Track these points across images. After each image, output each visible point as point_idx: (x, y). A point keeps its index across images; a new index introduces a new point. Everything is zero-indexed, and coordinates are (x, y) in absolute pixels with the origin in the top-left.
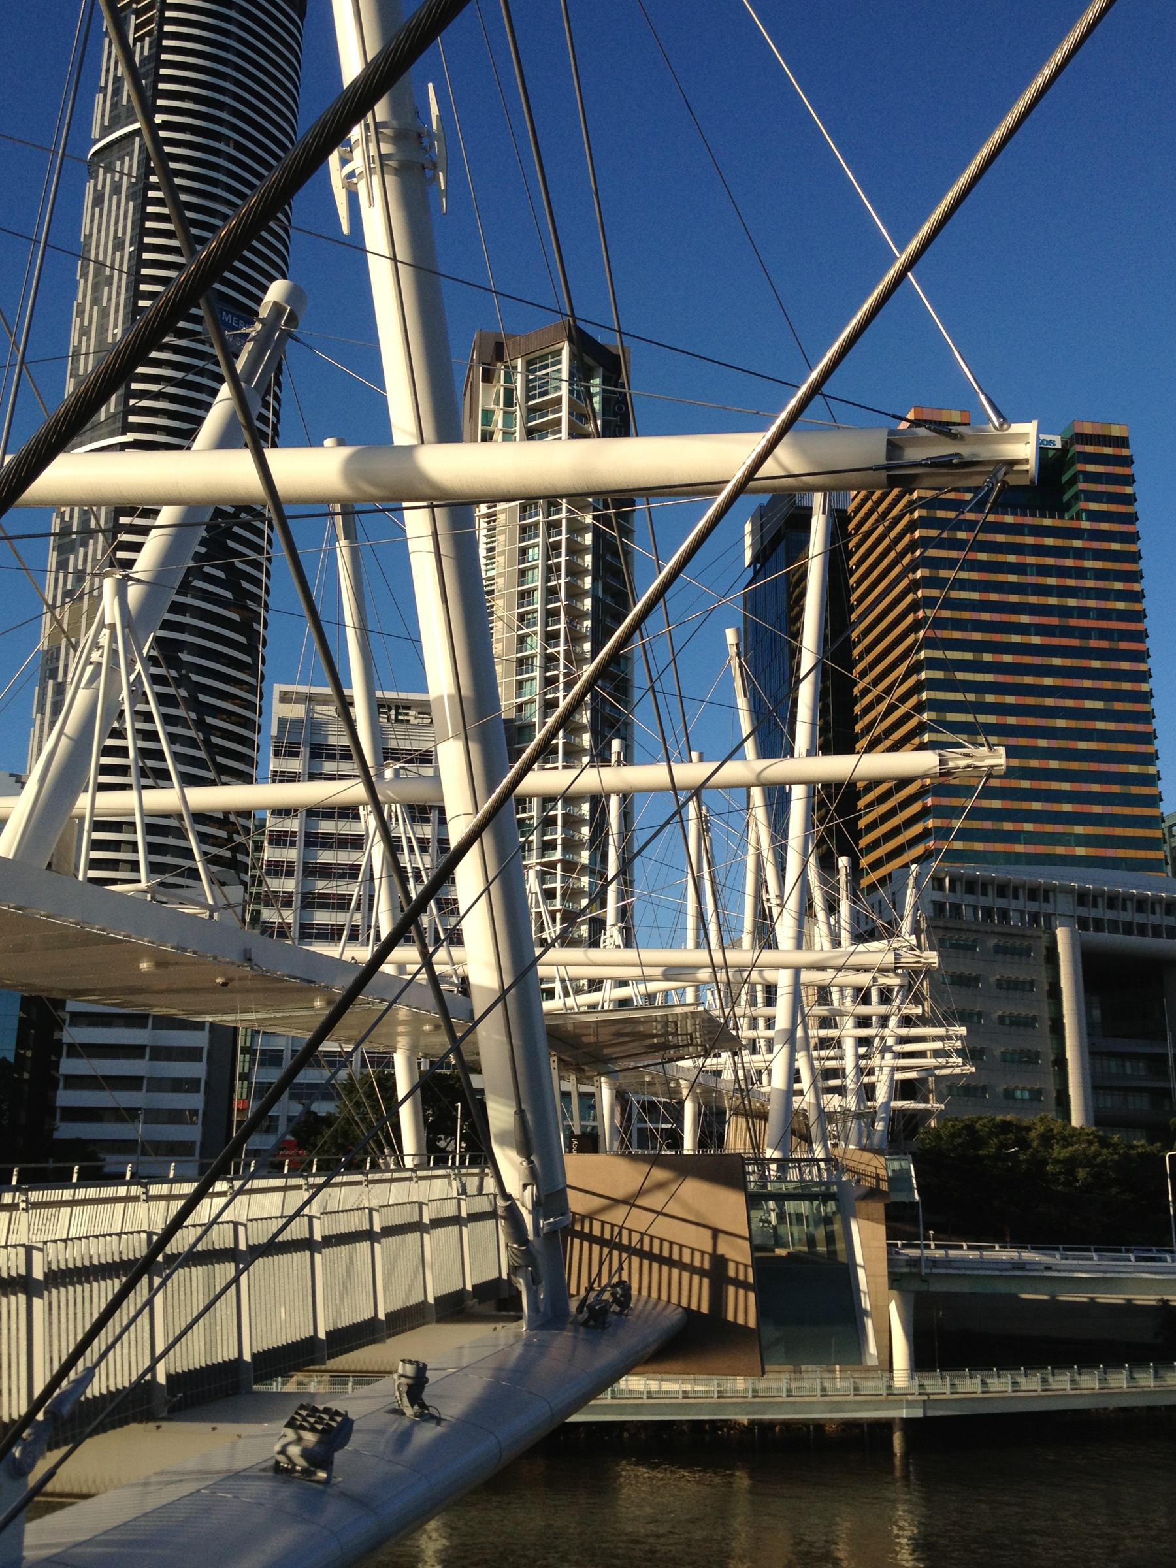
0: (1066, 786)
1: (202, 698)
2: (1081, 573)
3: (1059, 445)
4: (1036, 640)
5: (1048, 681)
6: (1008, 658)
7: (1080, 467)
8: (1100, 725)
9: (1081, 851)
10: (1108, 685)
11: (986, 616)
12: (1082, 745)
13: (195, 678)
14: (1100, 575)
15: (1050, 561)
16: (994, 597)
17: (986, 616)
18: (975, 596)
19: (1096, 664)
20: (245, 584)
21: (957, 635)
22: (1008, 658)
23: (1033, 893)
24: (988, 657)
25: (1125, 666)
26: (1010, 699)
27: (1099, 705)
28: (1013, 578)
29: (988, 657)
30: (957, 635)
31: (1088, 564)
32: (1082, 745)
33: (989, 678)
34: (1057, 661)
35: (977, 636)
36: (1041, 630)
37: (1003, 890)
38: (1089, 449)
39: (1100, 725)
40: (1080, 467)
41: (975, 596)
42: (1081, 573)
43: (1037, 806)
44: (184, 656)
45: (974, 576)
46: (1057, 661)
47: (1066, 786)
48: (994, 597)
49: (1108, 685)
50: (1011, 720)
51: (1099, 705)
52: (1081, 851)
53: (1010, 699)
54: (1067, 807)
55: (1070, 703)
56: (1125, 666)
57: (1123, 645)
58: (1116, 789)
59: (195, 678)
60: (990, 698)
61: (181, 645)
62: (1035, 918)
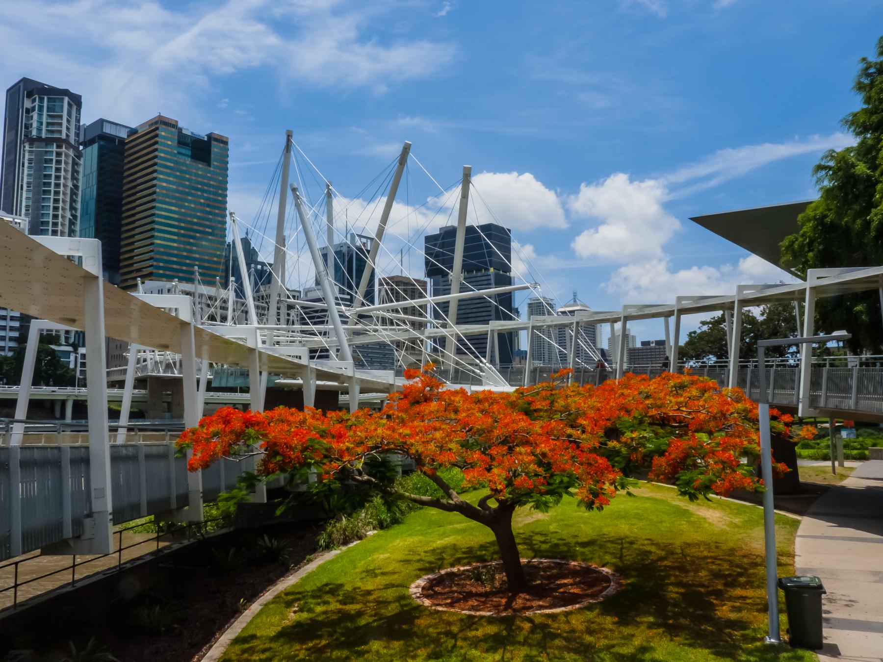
0: (197, 256)
4: (193, 206)
15: (200, 179)
21: (167, 200)
27: (210, 230)
28: (187, 183)
30: (167, 200)
33: (176, 216)
36: (195, 203)
42: (209, 185)
51: (210, 230)
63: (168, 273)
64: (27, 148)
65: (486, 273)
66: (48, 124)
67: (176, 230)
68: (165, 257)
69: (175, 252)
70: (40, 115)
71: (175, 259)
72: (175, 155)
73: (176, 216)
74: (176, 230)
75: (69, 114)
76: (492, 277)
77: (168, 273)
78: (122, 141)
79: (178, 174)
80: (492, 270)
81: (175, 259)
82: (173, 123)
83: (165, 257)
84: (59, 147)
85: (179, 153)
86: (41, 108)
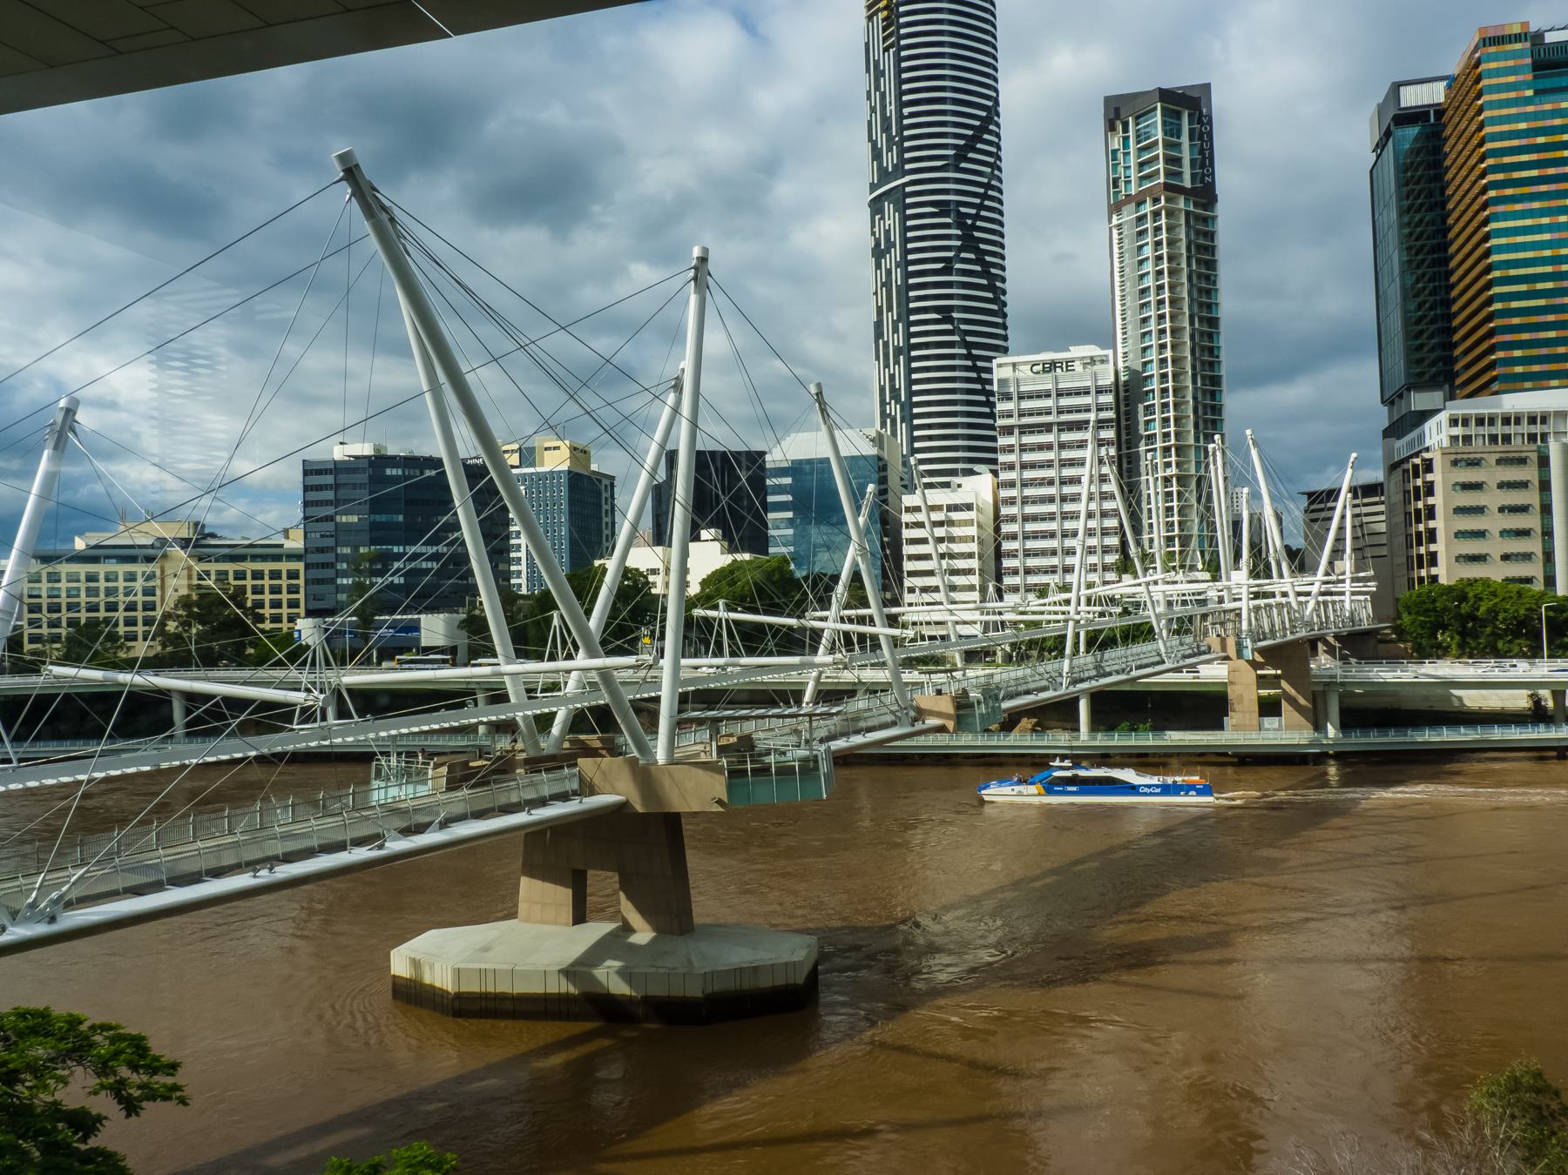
1: (969, 339)
11: (1544, 188)
13: (963, 327)
16: (1551, 171)
17: (1544, 188)
20: (988, 258)
23: (1532, 420)
33: (1547, 237)
37: (1506, 421)
41: (1534, 173)
44: (955, 315)
45: (1534, 157)
48: (1551, 171)
59: (963, 327)
61: (951, 309)
62: (1532, 438)
63: (1536, 368)
64: (1115, 221)
66: (1141, 165)
67: (1549, 269)
68: (1525, 336)
69: (1551, 318)
70: (1126, 154)
71: (1552, 334)
72: (1528, 101)
73: (1547, 237)
74: (1549, 269)
75: (1172, 130)
77: (1536, 368)
78: (1440, 111)
79: (1541, 140)
81: (1552, 334)
82: (1517, 30)
83: (1525, 336)
84: (1156, 201)
85: (1537, 92)
86: (1126, 139)
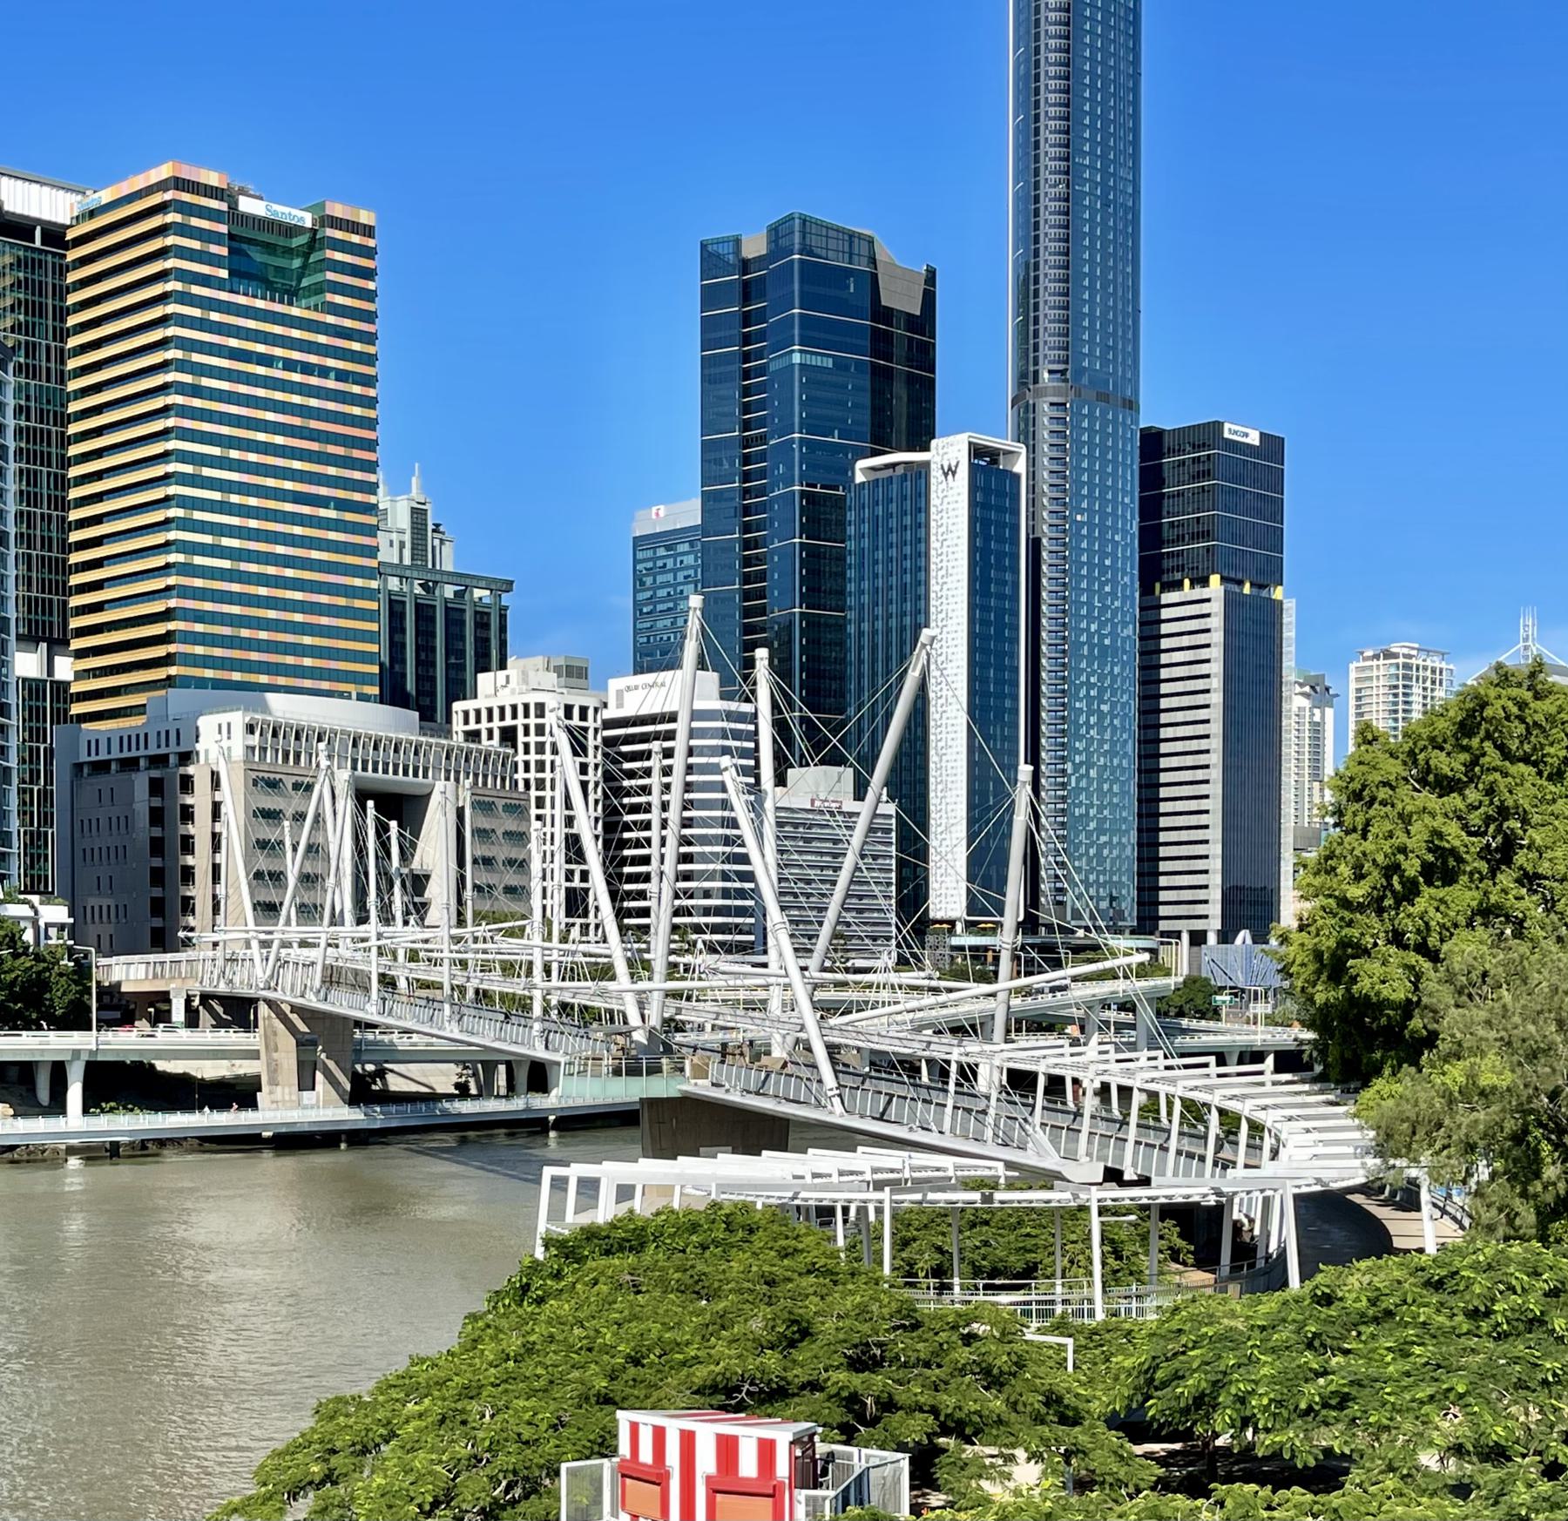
0: (298, 596)
2: (324, 372)
3: (308, 224)
5: (288, 485)
6: (252, 457)
7: (329, 254)
8: (332, 536)
9: (308, 662)
10: (340, 494)
12: (315, 555)
14: (342, 376)
18: (224, 385)
19: (332, 471)
22: (252, 457)
24: (234, 454)
25: (357, 475)
26: (253, 501)
29: (234, 454)
31: (331, 362)
32: (315, 555)
34: (297, 465)
35: (225, 430)
38: (339, 235)
39: (332, 536)
40: (329, 254)
41: (224, 385)
43: (272, 614)
46: (297, 465)
47: (298, 596)
49: (340, 494)
50: (253, 524)
52: (308, 662)
53: (253, 501)
54: (298, 617)
55: (306, 510)
56: (357, 475)
57: (356, 454)
58: (342, 601)
60: (235, 499)
65: (1199, 593)
76: (1216, 608)
80: (1215, 579)
81: (236, 610)
